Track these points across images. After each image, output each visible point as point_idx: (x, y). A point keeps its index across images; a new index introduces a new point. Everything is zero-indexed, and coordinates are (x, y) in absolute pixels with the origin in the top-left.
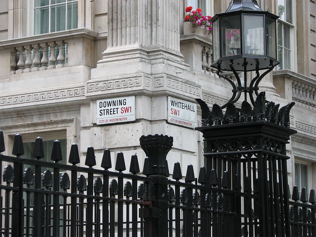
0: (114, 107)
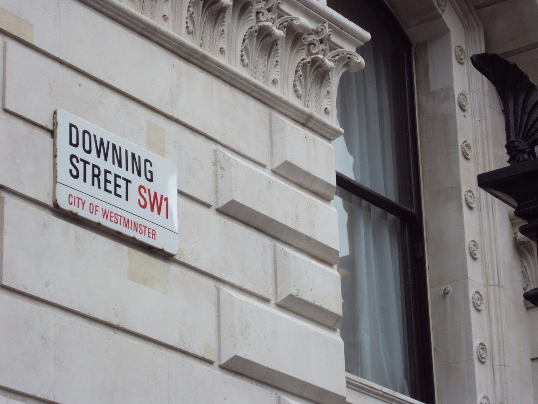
0: (115, 169)
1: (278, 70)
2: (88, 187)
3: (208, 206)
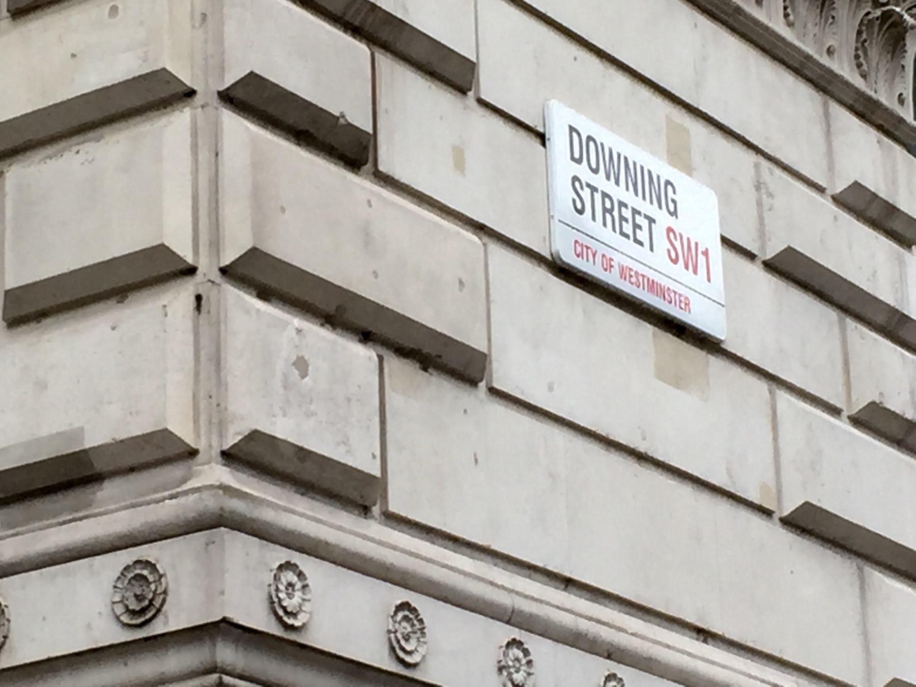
1: (834, 30)
2: (596, 228)
3: (751, 256)
